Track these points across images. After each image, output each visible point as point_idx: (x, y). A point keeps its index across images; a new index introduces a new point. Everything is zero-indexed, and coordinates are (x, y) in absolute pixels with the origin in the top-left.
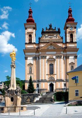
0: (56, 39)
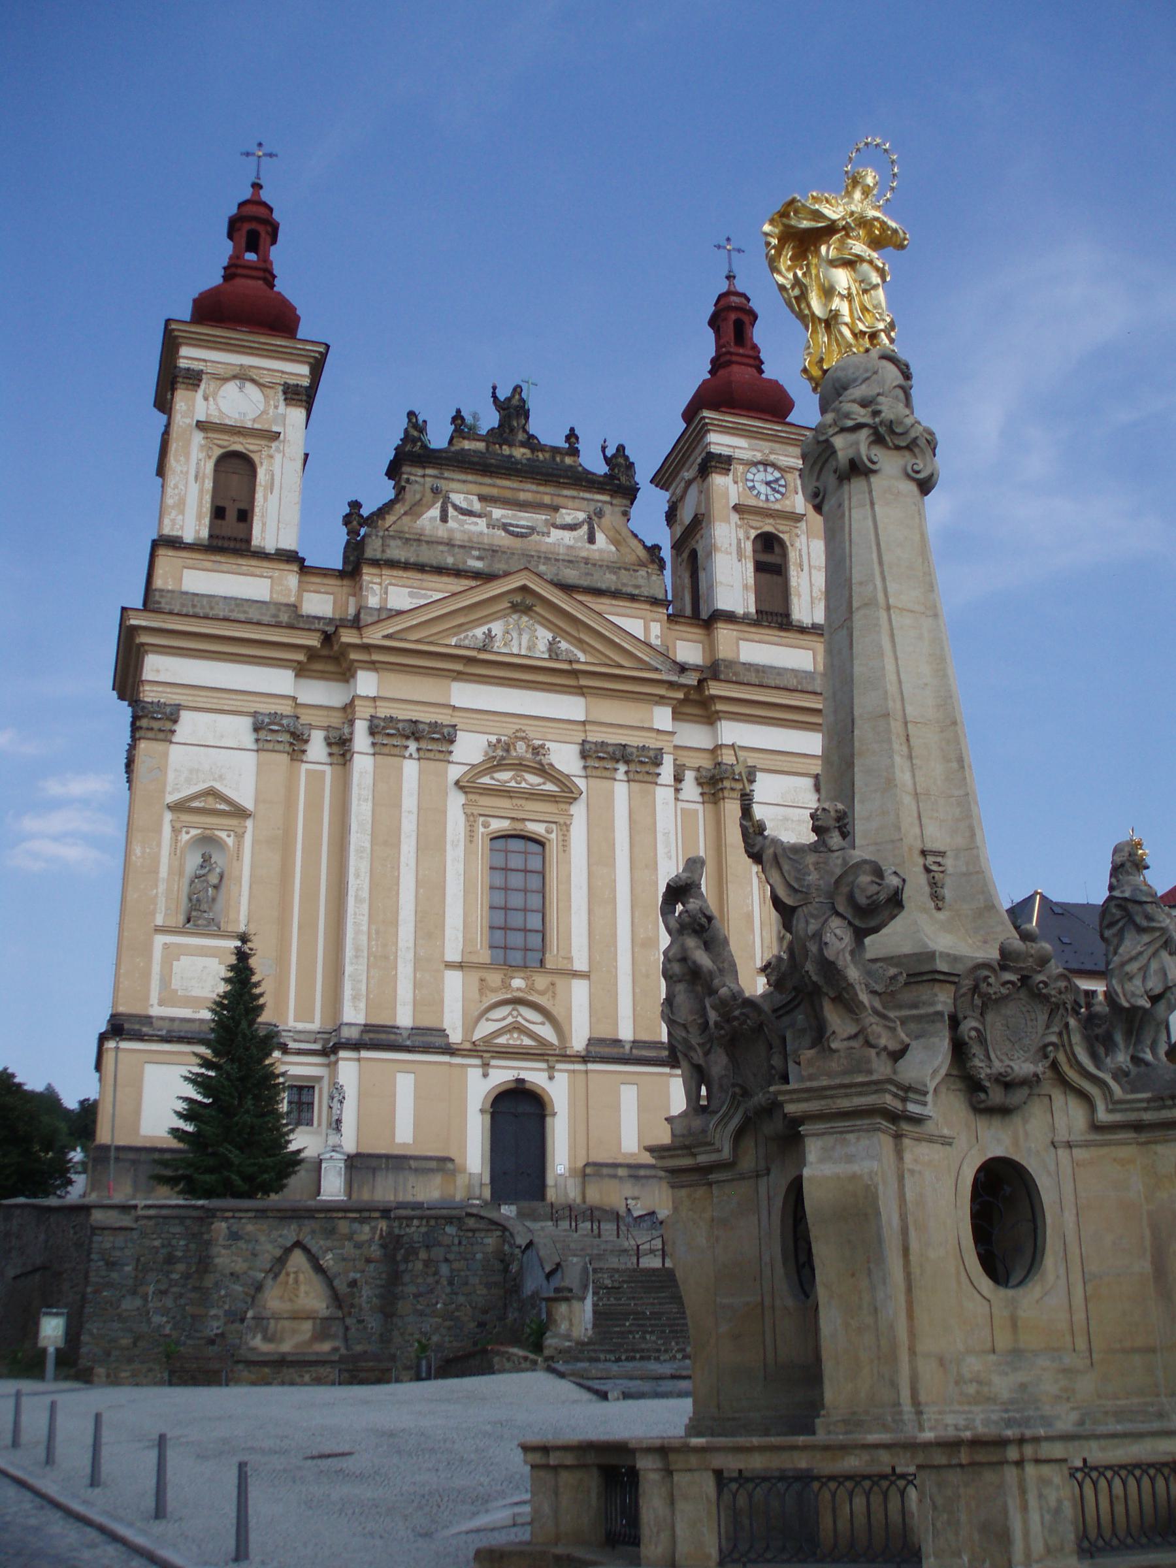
0: (587, 561)
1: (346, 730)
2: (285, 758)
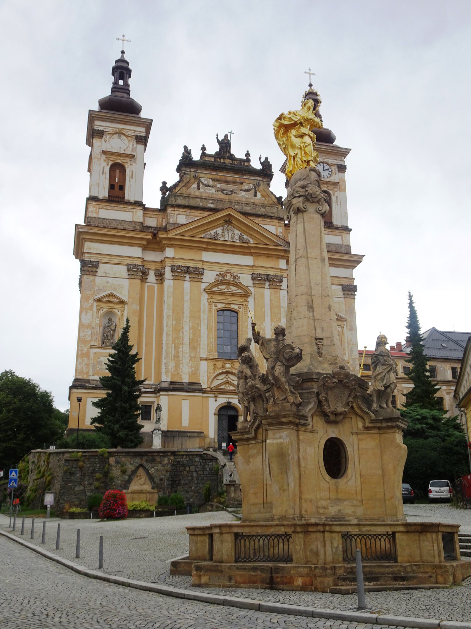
1: (162, 271)
2: (139, 281)
